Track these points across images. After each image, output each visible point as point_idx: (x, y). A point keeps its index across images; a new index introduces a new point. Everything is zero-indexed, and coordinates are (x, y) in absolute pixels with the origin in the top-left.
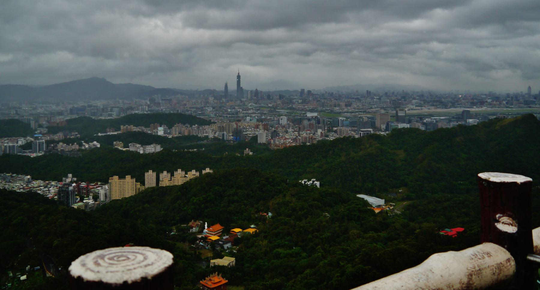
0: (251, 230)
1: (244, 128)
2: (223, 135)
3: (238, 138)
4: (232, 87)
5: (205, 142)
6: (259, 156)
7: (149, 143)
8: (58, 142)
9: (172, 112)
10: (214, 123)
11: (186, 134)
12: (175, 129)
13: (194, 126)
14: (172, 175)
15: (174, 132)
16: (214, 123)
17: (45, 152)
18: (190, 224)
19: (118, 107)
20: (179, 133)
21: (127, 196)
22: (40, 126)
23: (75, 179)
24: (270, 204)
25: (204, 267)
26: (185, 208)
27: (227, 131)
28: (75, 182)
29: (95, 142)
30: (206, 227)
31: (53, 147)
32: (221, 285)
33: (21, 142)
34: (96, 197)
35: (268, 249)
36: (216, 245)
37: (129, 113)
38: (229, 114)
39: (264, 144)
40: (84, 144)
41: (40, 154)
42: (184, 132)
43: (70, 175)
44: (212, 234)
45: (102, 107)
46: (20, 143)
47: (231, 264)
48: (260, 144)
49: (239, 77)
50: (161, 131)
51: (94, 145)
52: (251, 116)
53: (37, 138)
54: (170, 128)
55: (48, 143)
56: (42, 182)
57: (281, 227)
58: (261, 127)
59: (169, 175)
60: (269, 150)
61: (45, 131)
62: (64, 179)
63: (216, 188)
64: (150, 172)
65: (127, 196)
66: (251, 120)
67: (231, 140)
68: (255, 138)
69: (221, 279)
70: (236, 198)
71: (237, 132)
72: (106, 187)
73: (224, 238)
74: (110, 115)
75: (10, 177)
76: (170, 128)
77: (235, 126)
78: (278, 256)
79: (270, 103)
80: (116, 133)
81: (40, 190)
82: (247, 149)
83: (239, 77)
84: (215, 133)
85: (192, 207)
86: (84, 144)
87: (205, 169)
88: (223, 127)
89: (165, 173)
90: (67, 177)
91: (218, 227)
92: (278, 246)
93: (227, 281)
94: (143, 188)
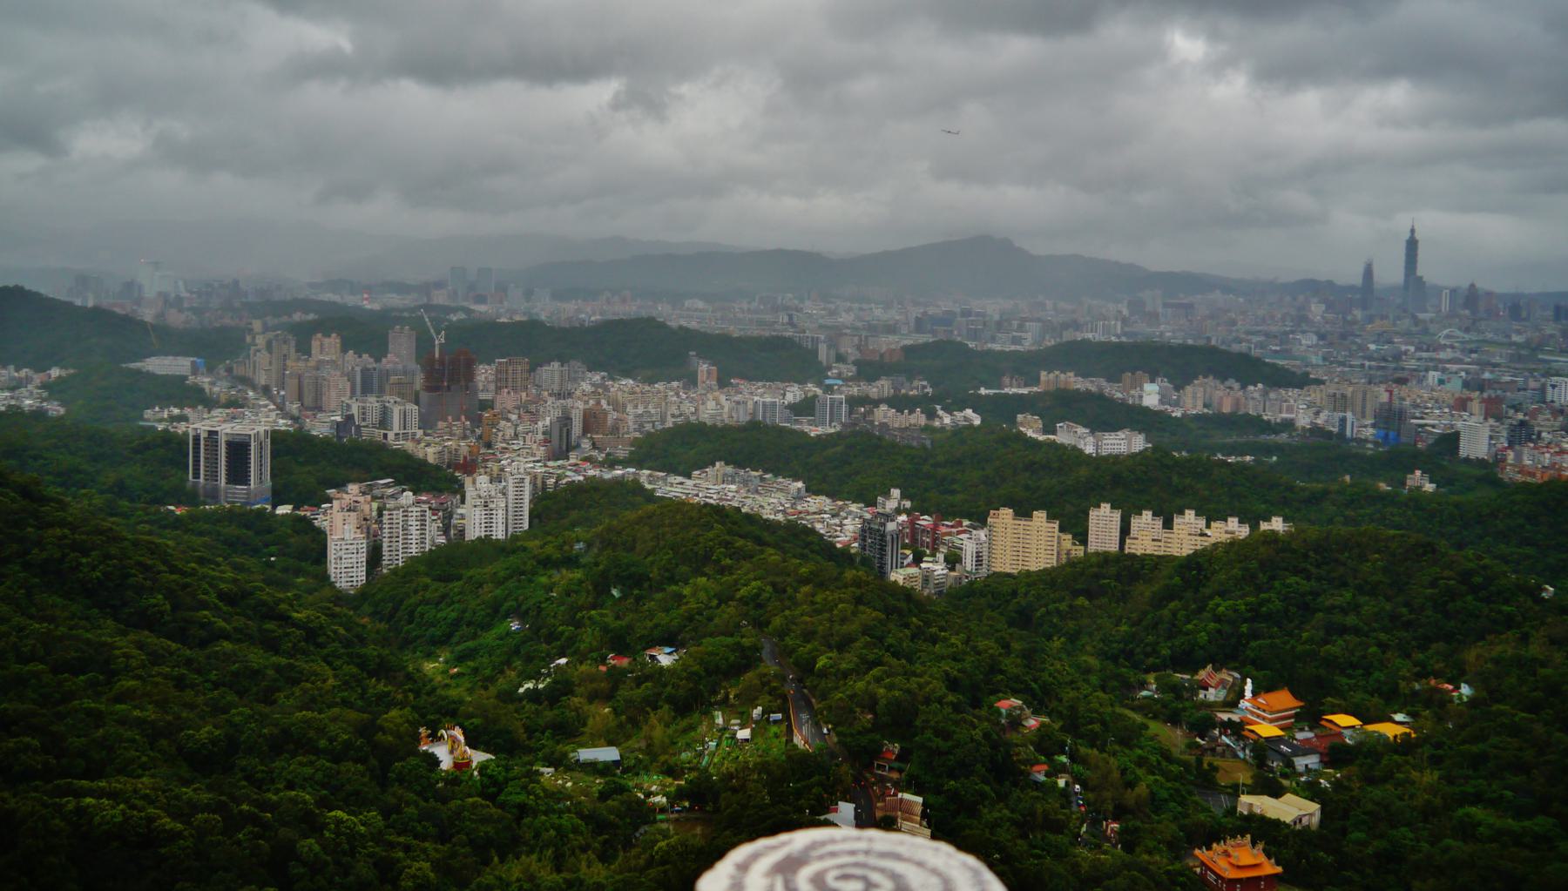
0: (1389, 730)
1: (1416, 406)
2: (1343, 421)
3: (1392, 434)
4: (1390, 273)
5: (1283, 437)
6: (1455, 498)
7: (1113, 427)
8: (876, 403)
9: (1190, 342)
10: (1319, 382)
11: (1227, 409)
12: (1195, 394)
13: (1251, 388)
14: (1168, 525)
15: (1188, 401)
16: (1319, 382)
17: (843, 425)
18: (1202, 674)
19: (1039, 320)
20: (1205, 406)
21: (1033, 568)
22: (841, 358)
23: (908, 504)
24: (1471, 655)
25: (1218, 812)
26: (1190, 627)
27: (1359, 409)
28: (906, 511)
29: (969, 412)
30: (1248, 694)
31: (864, 415)
32: (1259, 878)
33: (794, 394)
34: (953, 560)
35: (1438, 801)
36: (1269, 753)
37: (1068, 336)
38: (1370, 359)
39: (1481, 463)
40: (940, 413)
42: (1220, 404)
43: (896, 493)
44: (1264, 719)
45: (997, 317)
46: (790, 398)
47: (1305, 821)
48: (1467, 460)
49: (1412, 245)
50: (1151, 395)
51: (966, 419)
52: (1444, 370)
53: (829, 389)
54: (1178, 388)
55: (853, 402)
56: (828, 501)
57: (1494, 740)
58: (1476, 406)
59: (1159, 523)
60: (1496, 483)
61: (849, 370)
62: (880, 499)
63: (1292, 580)
64: (1106, 508)
65: (1034, 567)
66: (1441, 382)
67: (1366, 441)
68: (1451, 440)
69: (1263, 859)
70: (1351, 620)
71: (1390, 417)
72: (982, 534)
73: (1300, 736)
74: (1016, 341)
75: (757, 481)
76: (1178, 388)
77: (1385, 397)
78: (1467, 830)
79: (1519, 332)
80: (1025, 391)
81: (822, 521)
82: (1418, 473)
83: (1412, 245)
84: (1317, 414)
85: (1212, 625)
86: (940, 413)
87: (1268, 520)
88: (1344, 396)
89: (1147, 515)
90: (887, 495)
91: (1284, 700)
92: (1477, 799)
93: (1279, 869)
94: (1079, 551)
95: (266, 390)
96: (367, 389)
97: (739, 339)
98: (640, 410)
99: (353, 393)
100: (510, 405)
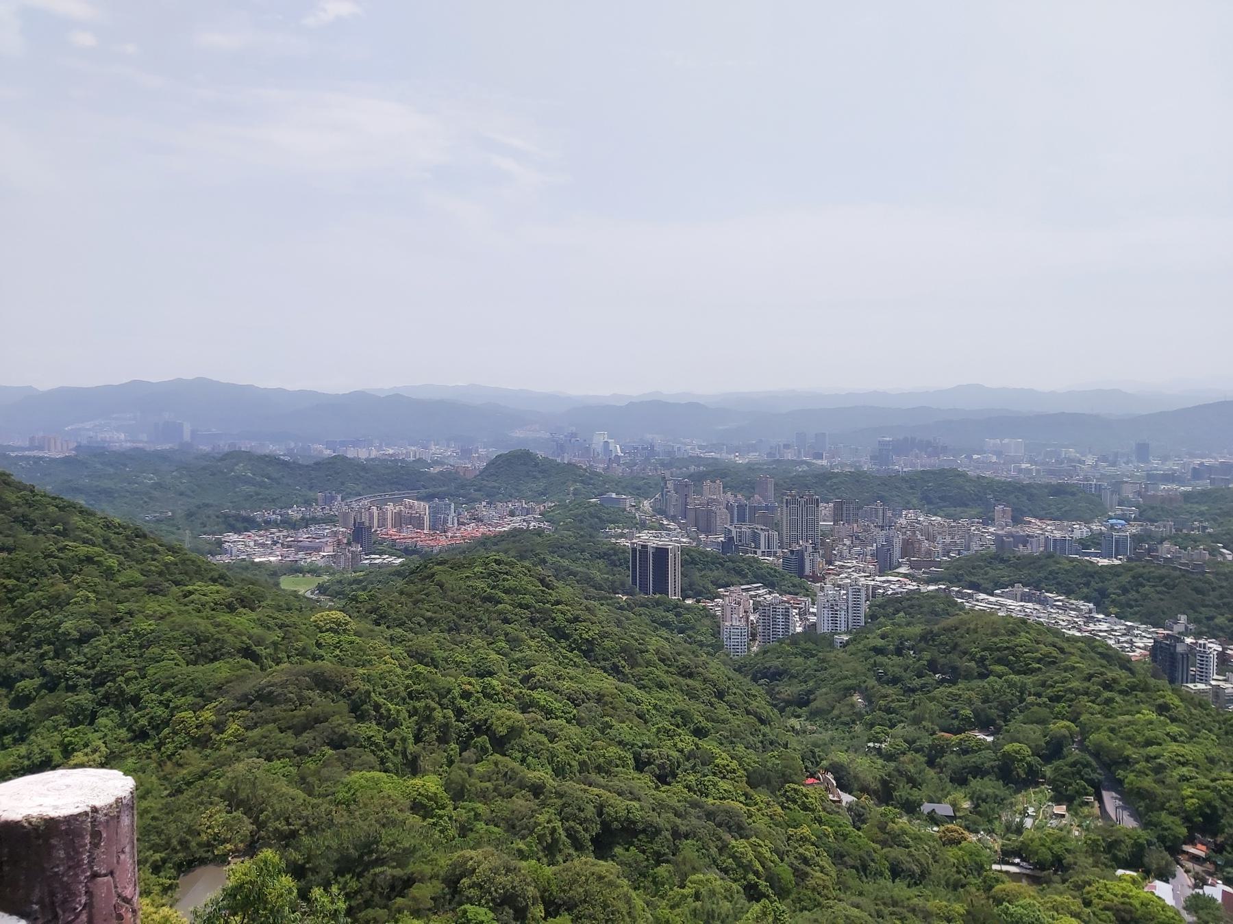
17: (1129, 559)
31: (1149, 551)
33: (1080, 531)
41: (1117, 562)
43: (1183, 619)
46: (1077, 534)
61: (1133, 512)
95: (673, 519)
96: (742, 519)
97: (1029, 486)
98: (948, 540)
99: (732, 521)
100: (843, 534)
